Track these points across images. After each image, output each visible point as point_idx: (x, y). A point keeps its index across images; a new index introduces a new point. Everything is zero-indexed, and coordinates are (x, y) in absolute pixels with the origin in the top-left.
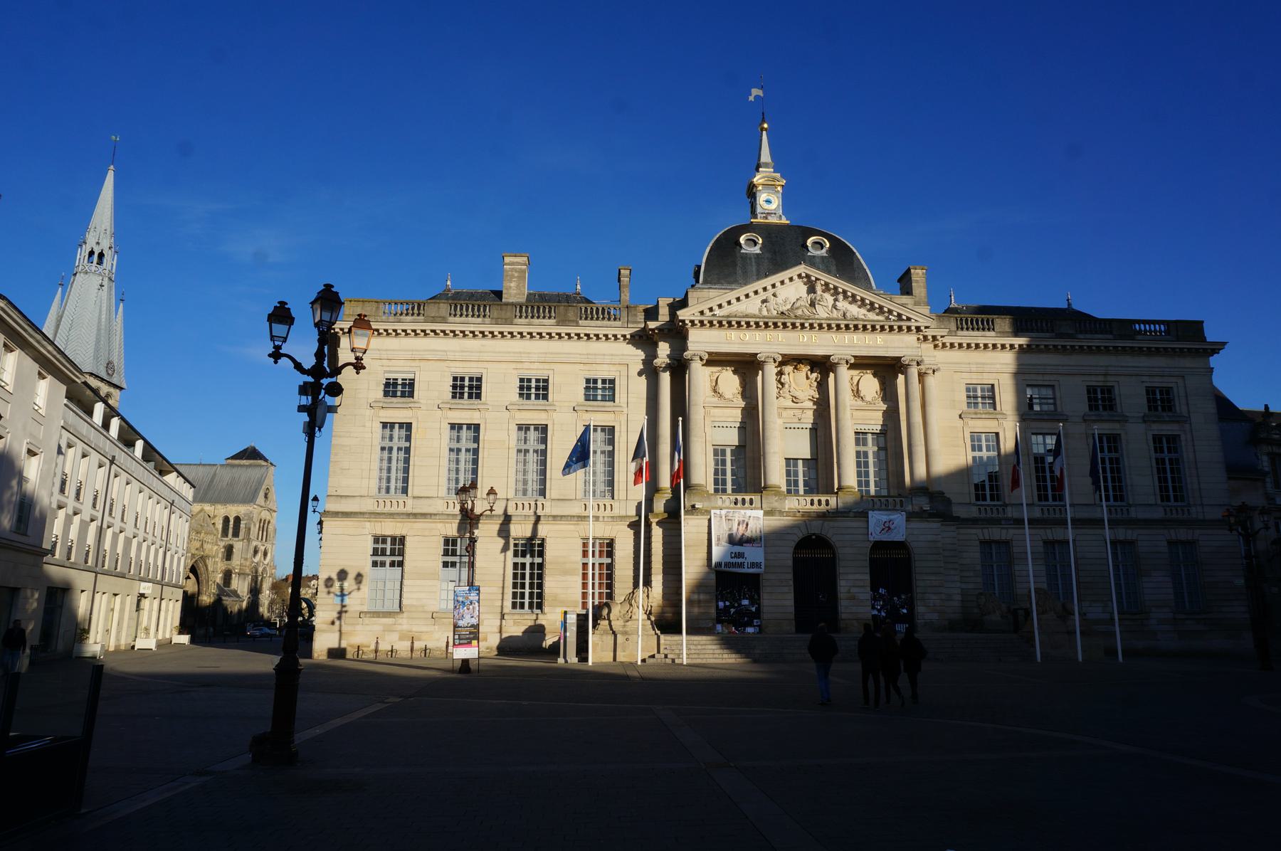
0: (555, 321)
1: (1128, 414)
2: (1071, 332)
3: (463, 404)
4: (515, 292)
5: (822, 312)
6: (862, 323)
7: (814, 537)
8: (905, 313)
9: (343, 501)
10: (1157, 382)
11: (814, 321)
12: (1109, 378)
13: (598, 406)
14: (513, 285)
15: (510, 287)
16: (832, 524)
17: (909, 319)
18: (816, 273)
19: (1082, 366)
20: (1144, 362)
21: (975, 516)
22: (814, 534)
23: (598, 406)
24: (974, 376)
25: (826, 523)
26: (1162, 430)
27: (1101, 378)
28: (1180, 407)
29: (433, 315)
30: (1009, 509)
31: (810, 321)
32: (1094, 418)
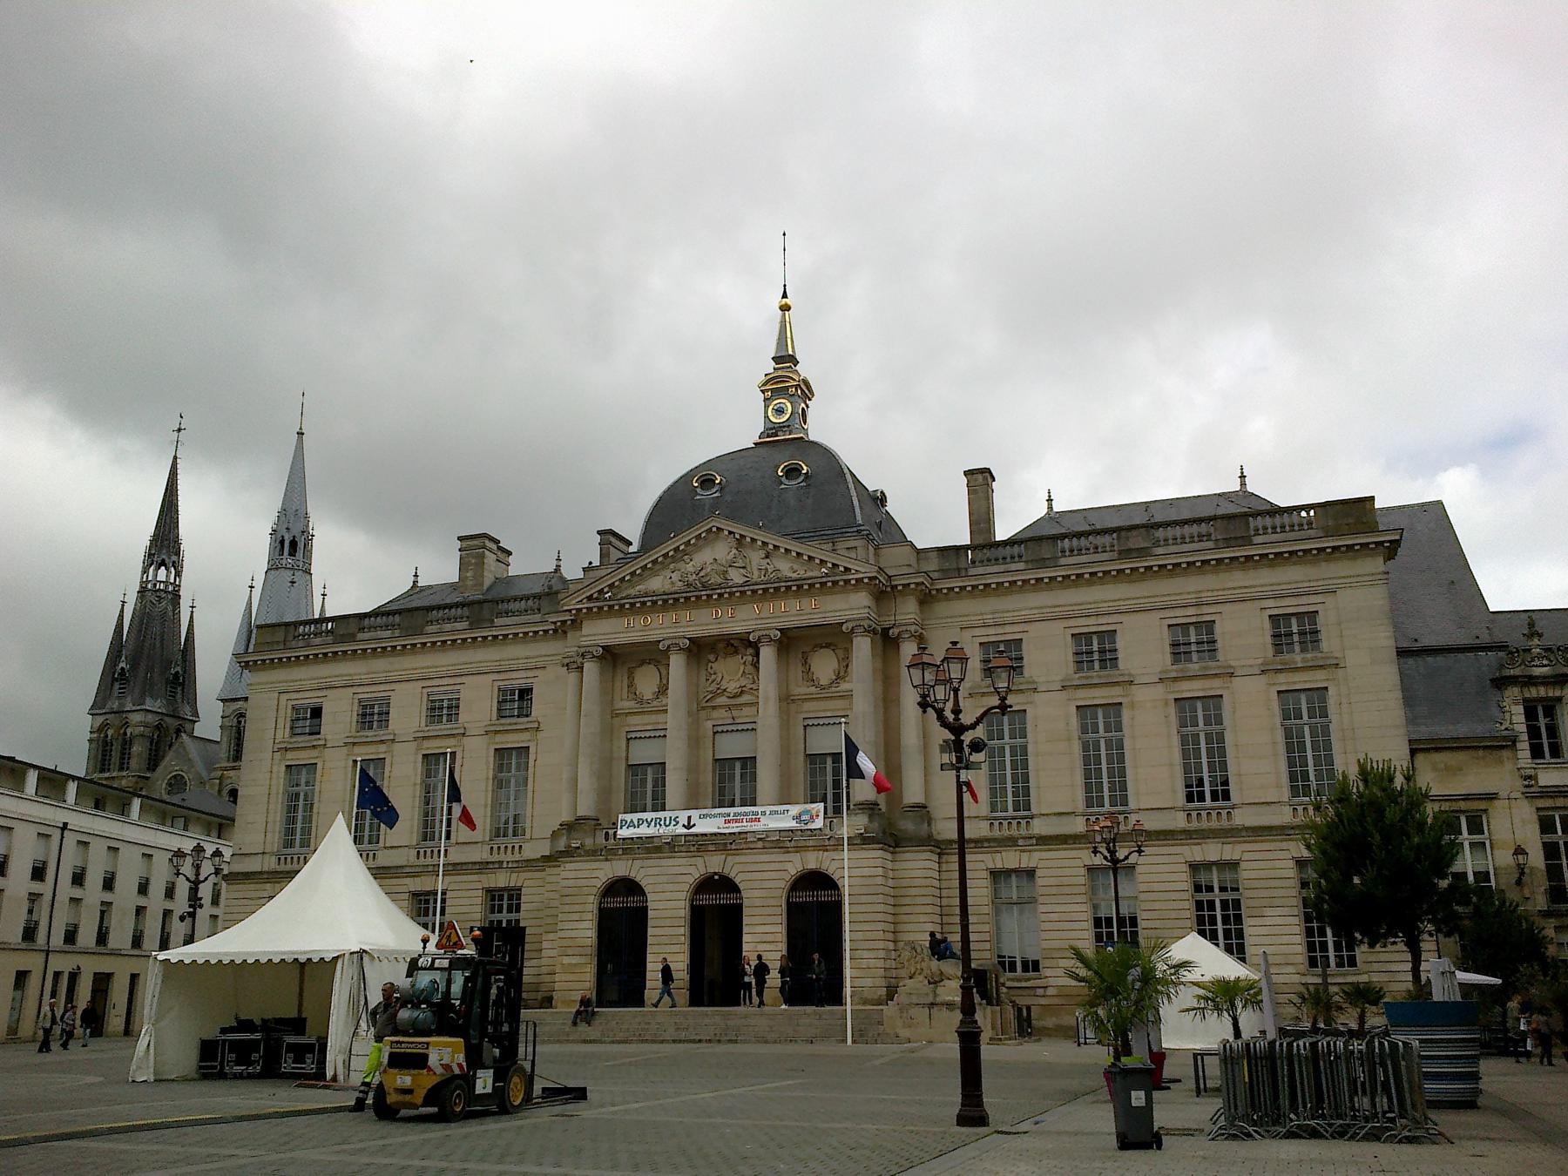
0: (467, 623)
1: (1233, 663)
2: (1146, 545)
3: (367, 737)
4: (471, 583)
5: (736, 577)
6: (783, 584)
7: (716, 877)
8: (843, 563)
9: (247, 859)
10: (1289, 606)
11: (723, 591)
12: (1206, 610)
13: (510, 724)
14: (468, 574)
15: (467, 577)
16: (738, 859)
17: (847, 570)
18: (728, 525)
19: (1246, 587)
20: (1264, 578)
21: (986, 834)
22: (716, 874)
23: (510, 724)
24: (992, 631)
25: (730, 858)
26: (1295, 683)
27: (1191, 611)
28: (1329, 643)
29: (341, 633)
30: (1035, 822)
31: (719, 591)
32: (1174, 675)
